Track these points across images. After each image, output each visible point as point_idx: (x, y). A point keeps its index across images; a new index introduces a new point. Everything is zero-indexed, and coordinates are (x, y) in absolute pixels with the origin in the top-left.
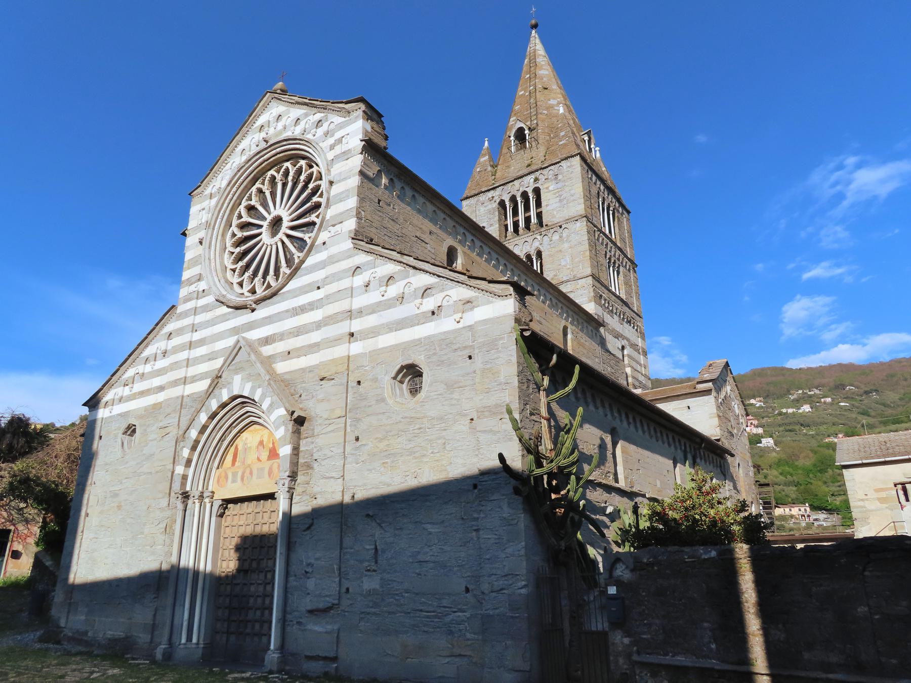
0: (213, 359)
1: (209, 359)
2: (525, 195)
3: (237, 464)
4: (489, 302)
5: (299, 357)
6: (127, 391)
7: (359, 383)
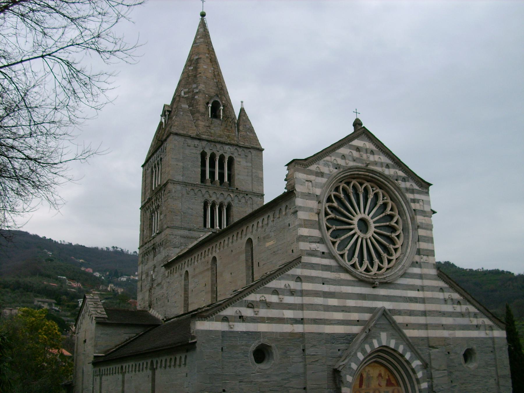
0: (346, 312)
1: (343, 311)
2: (222, 158)
3: (364, 387)
4: (498, 330)
5: (414, 329)
6: (248, 312)
7: (449, 353)
